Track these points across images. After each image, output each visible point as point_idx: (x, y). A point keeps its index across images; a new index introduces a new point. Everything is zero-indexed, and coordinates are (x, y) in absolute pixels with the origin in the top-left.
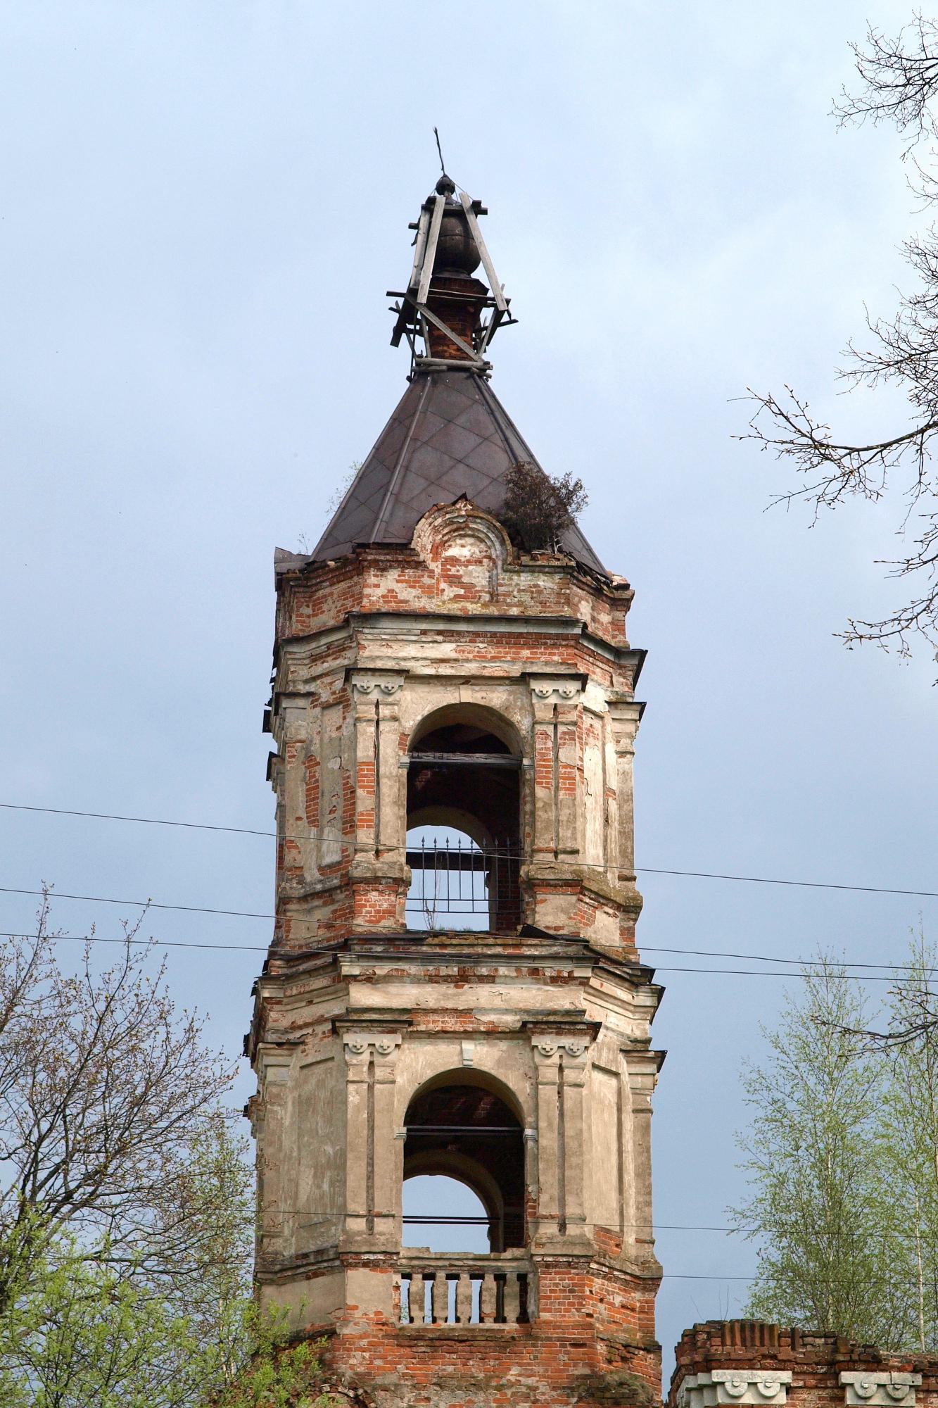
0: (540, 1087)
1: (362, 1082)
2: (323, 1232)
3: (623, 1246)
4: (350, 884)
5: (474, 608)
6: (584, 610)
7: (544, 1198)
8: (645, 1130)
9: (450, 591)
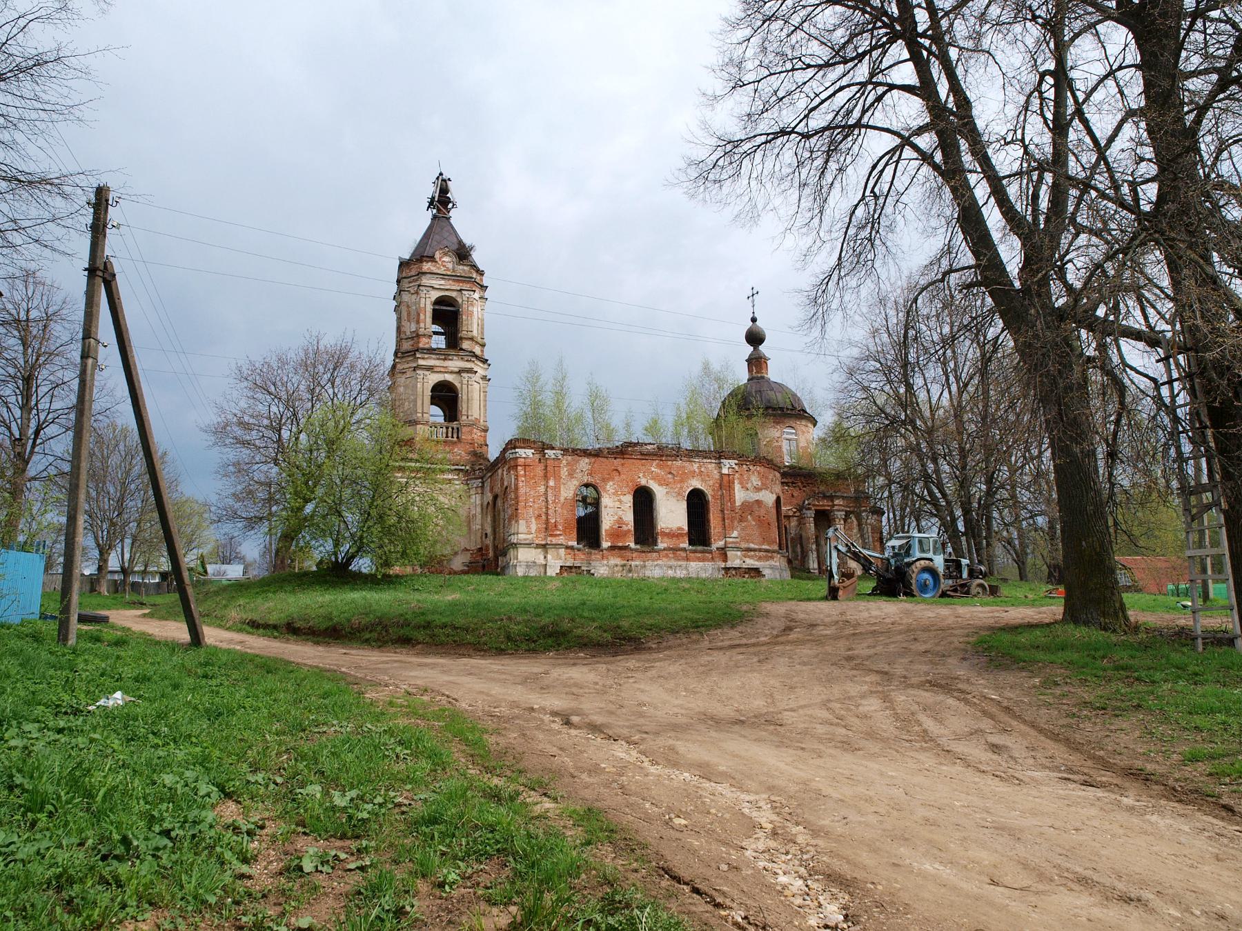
4: (418, 336)
5: (449, 273)
6: (474, 275)
8: (485, 396)
9: (443, 269)
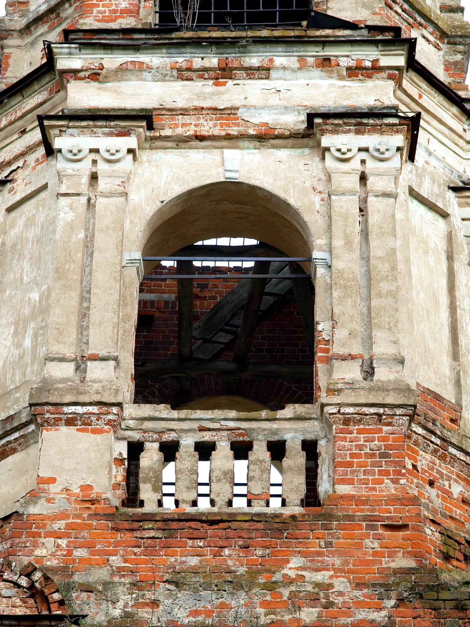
0: (333, 197)
1: (78, 195)
2: (19, 398)
3: (461, 423)
7: (341, 334)
